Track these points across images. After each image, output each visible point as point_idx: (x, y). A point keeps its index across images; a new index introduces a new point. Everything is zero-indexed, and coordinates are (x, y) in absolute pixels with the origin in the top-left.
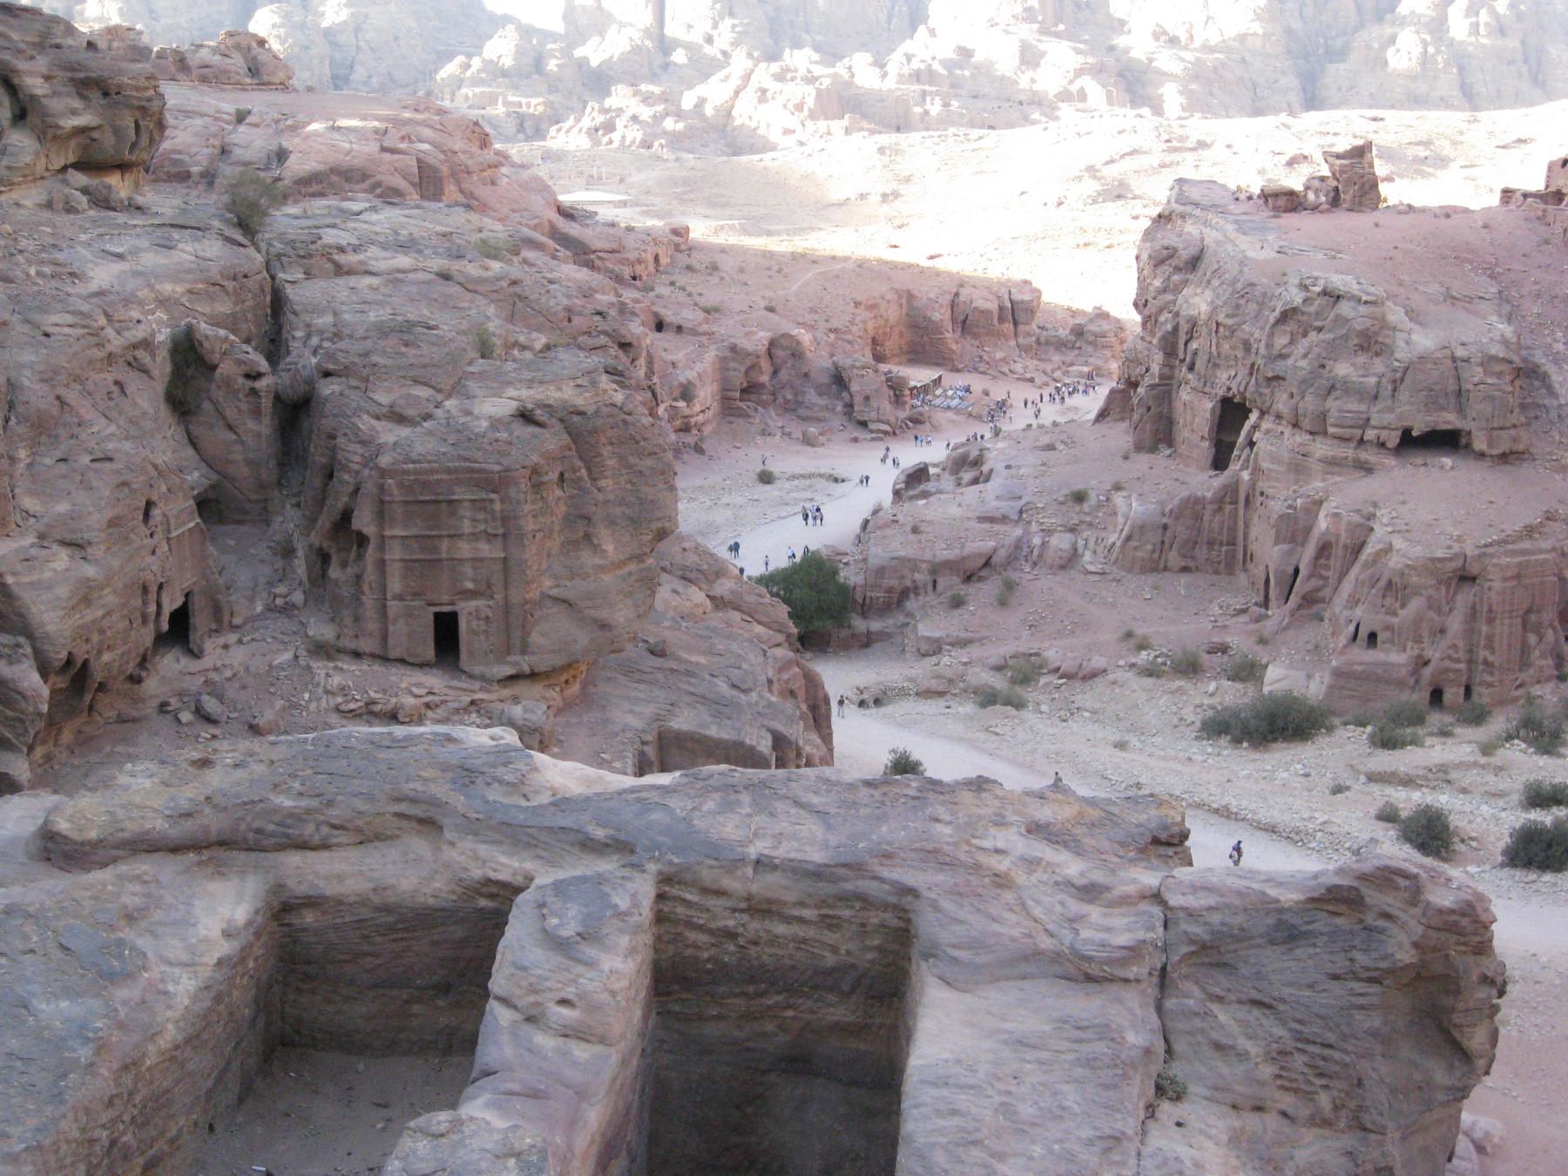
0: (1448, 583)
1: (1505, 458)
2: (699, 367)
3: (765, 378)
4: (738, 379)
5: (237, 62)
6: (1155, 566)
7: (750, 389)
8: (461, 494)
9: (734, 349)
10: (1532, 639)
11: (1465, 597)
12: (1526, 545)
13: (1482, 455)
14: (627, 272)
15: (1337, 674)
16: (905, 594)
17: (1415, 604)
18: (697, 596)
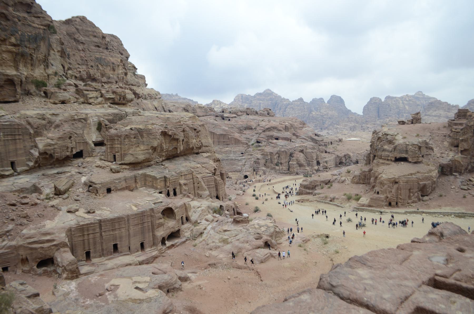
0: (392, 183)
1: (416, 163)
2: (330, 158)
3: (344, 161)
4: (338, 161)
5: (266, 113)
6: (357, 183)
7: (340, 163)
8: (116, 138)
9: (338, 156)
10: (412, 194)
11: (396, 186)
12: (410, 177)
13: (410, 162)
14: (323, 144)
15: (371, 199)
16: (315, 186)
17: (386, 186)
18: (199, 165)
